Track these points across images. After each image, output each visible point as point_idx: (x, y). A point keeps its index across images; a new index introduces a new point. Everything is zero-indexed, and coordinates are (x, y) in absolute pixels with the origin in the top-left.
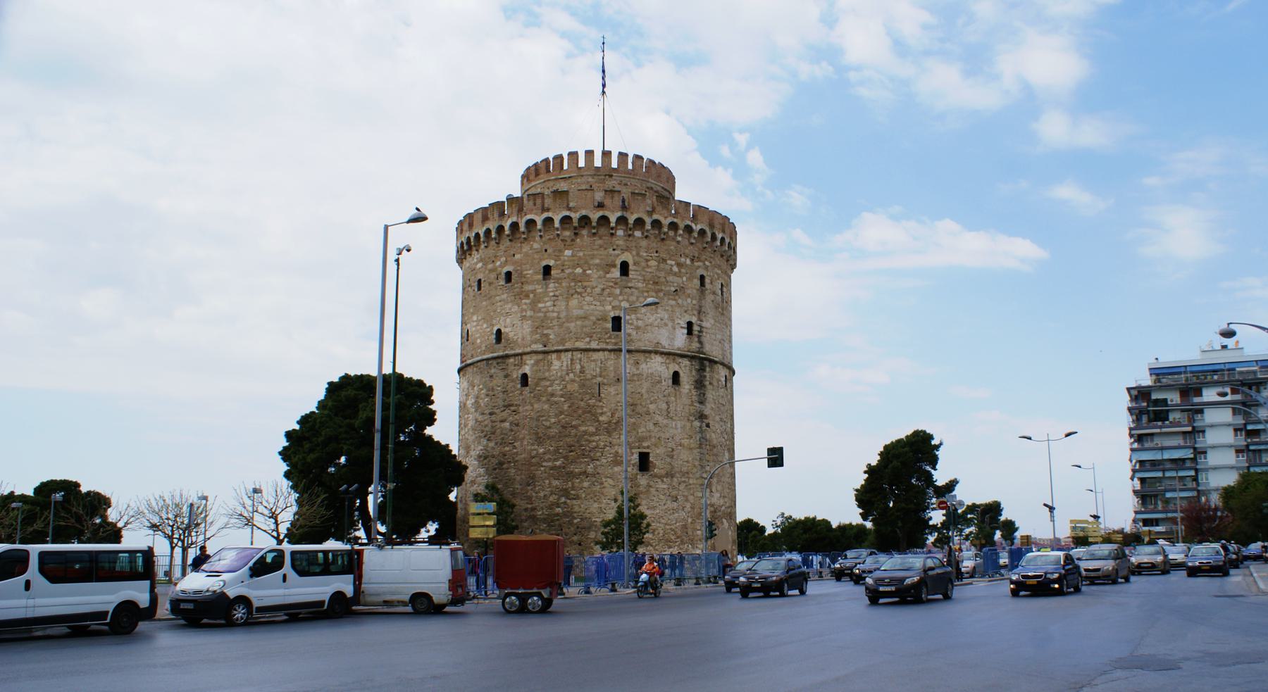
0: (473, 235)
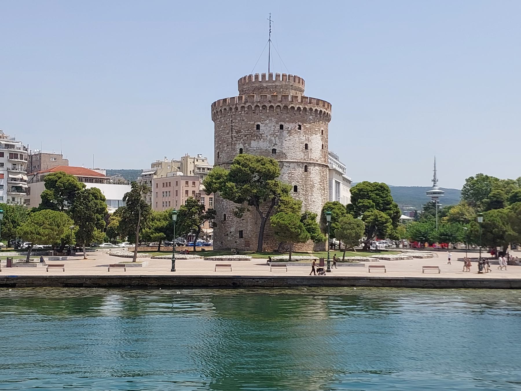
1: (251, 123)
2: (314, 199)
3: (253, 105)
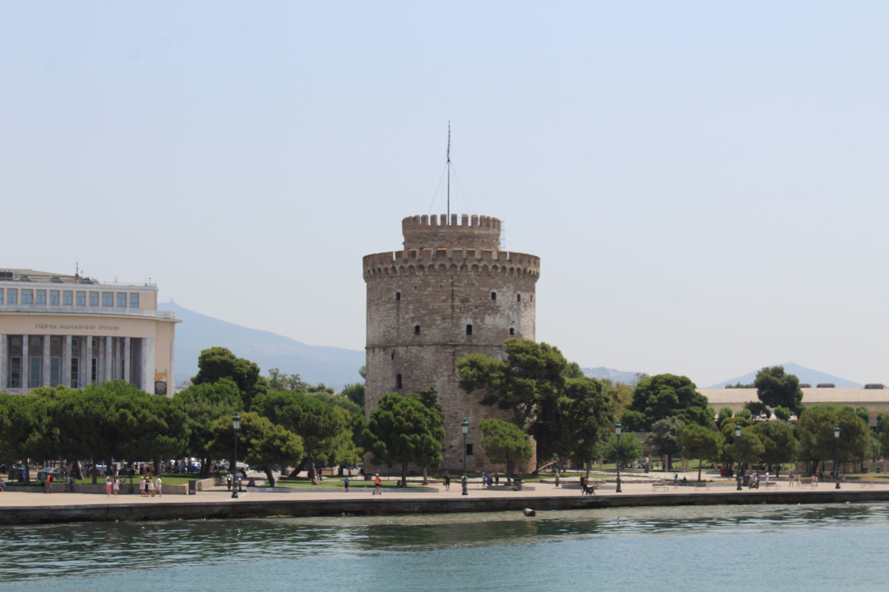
1: (486, 289)
3: (490, 264)
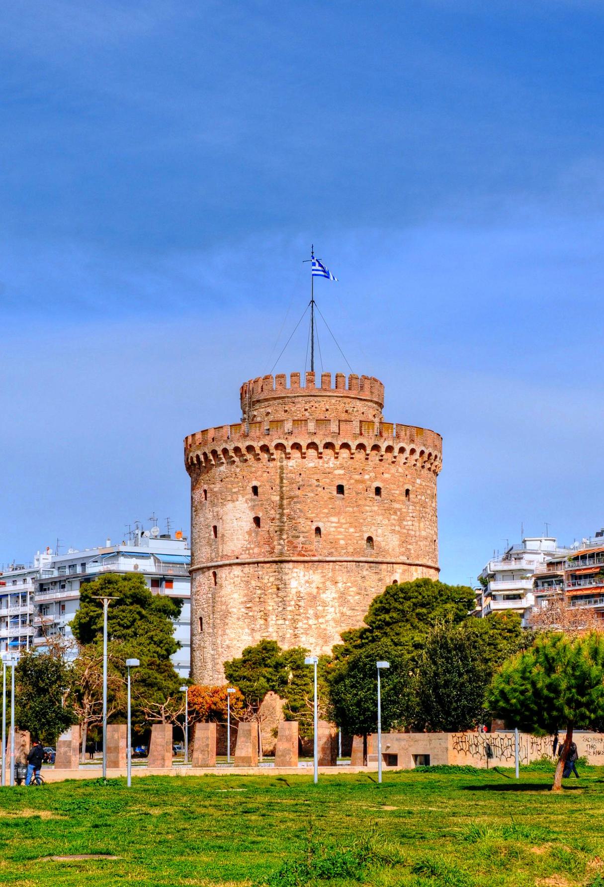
0: (340, 443)
2: (227, 642)
